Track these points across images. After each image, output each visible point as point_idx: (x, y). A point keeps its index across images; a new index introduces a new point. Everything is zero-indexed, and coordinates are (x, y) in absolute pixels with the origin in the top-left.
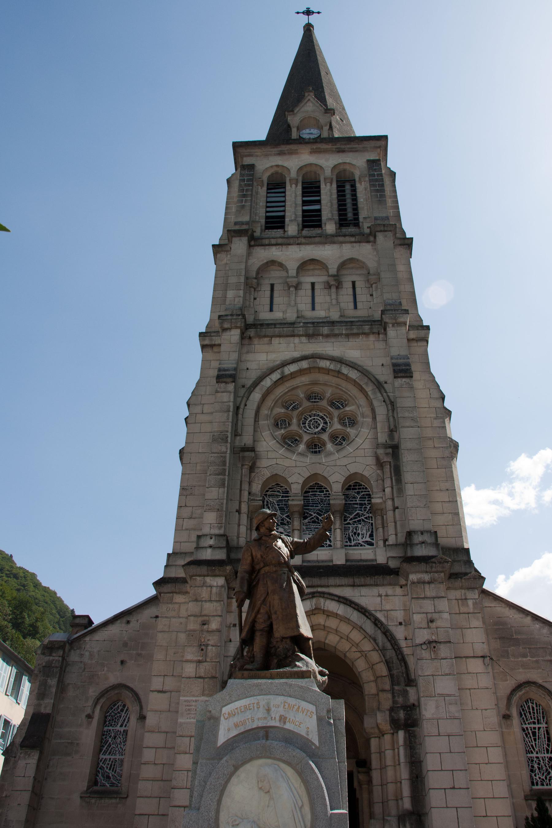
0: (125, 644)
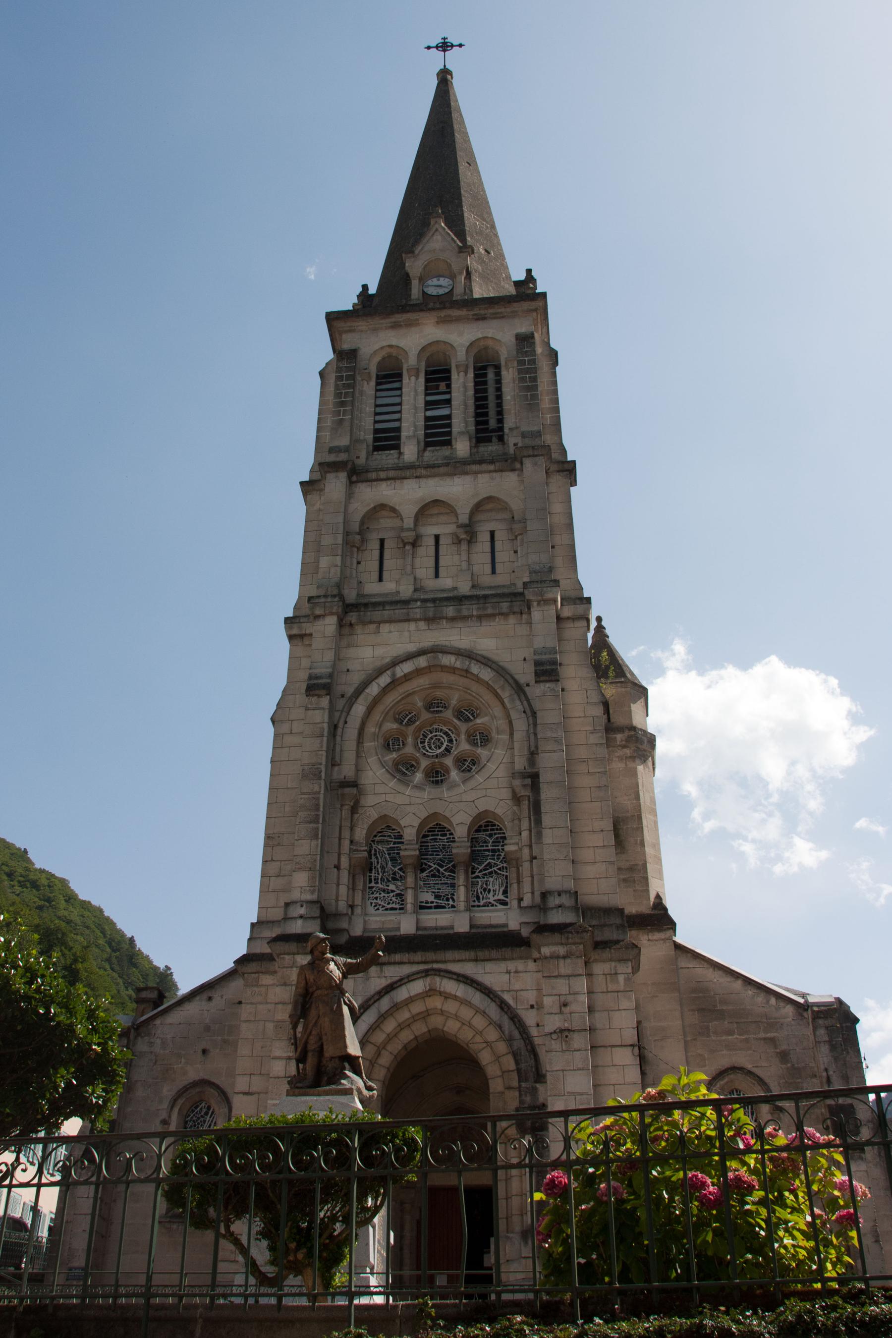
0: (207, 1029)
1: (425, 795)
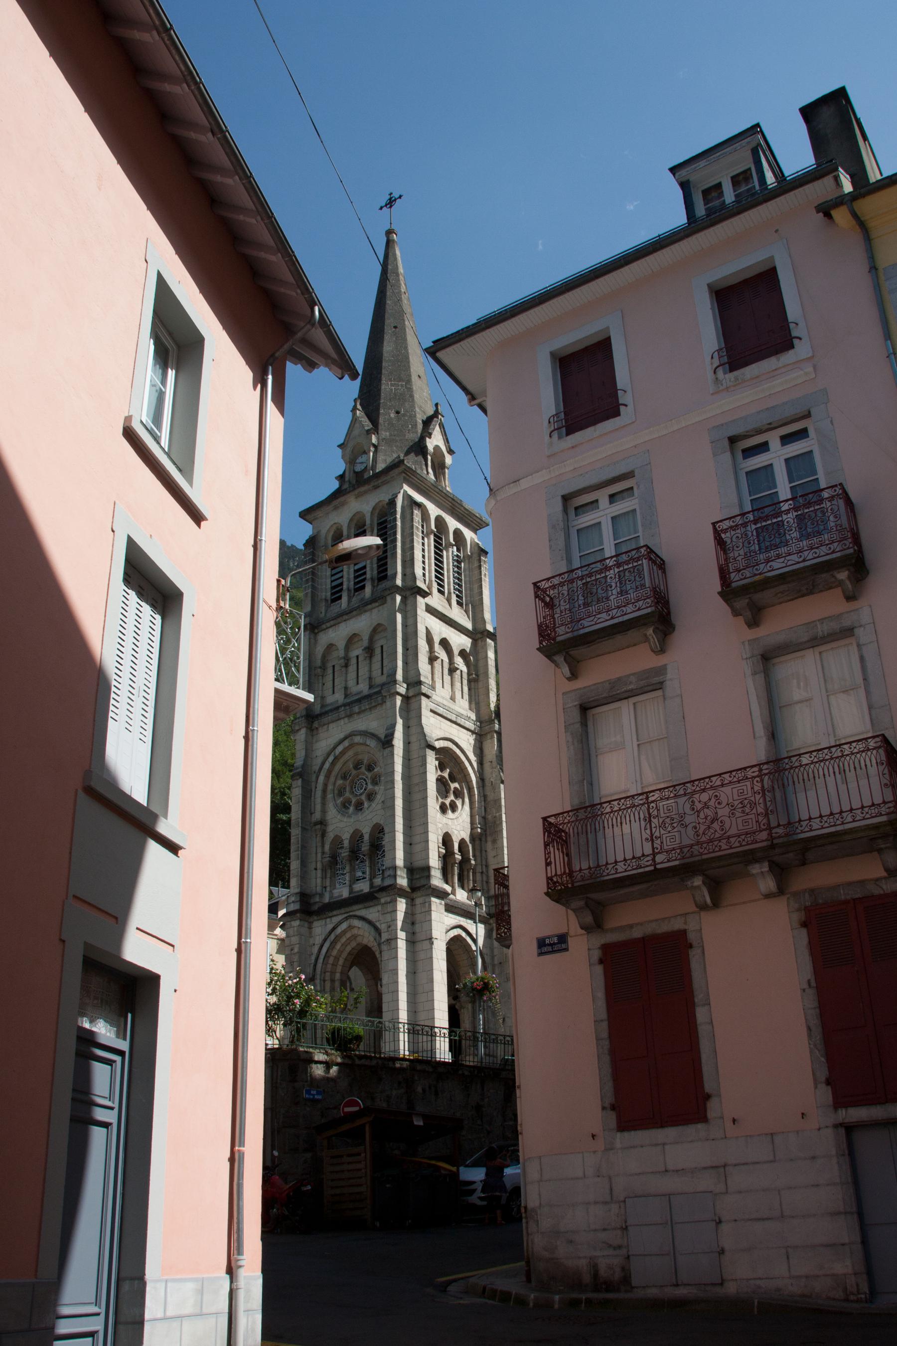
1: (352, 820)
